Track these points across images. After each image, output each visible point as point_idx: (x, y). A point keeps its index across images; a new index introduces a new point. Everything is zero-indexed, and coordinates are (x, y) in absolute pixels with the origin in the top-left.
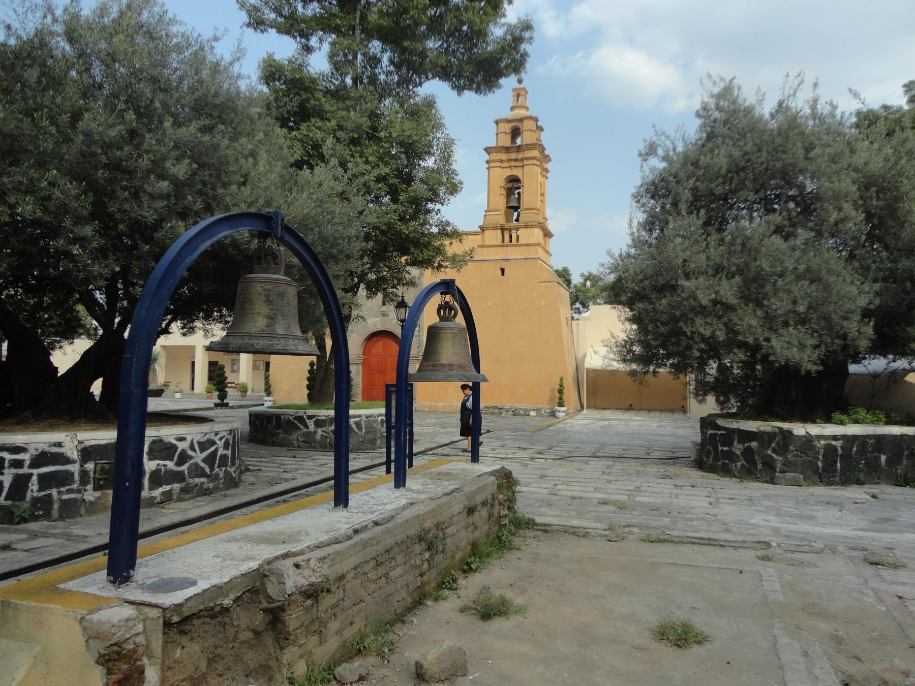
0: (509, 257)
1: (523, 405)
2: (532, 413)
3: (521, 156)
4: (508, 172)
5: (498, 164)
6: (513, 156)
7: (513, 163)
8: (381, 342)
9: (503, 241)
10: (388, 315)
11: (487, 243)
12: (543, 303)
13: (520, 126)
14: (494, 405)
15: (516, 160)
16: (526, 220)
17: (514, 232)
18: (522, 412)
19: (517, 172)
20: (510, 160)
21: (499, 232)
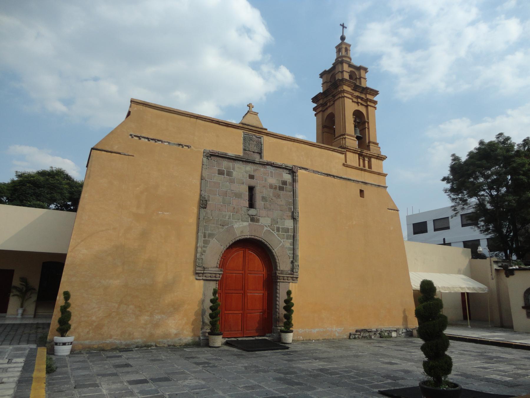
0: (367, 181)
1: (385, 326)
2: (394, 334)
3: (363, 96)
4: (355, 107)
5: (350, 96)
6: (357, 94)
7: (359, 101)
8: (241, 252)
9: (359, 165)
10: (258, 221)
11: (349, 163)
12: (392, 228)
13: (357, 73)
14: (363, 328)
15: (362, 99)
16: (375, 152)
17: (366, 159)
18: (386, 334)
19: (363, 109)
20: (357, 97)
21: (357, 155)
